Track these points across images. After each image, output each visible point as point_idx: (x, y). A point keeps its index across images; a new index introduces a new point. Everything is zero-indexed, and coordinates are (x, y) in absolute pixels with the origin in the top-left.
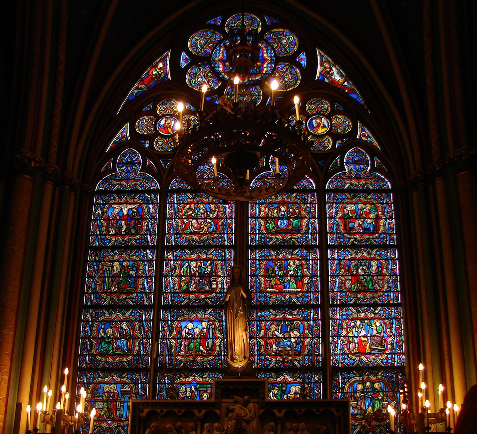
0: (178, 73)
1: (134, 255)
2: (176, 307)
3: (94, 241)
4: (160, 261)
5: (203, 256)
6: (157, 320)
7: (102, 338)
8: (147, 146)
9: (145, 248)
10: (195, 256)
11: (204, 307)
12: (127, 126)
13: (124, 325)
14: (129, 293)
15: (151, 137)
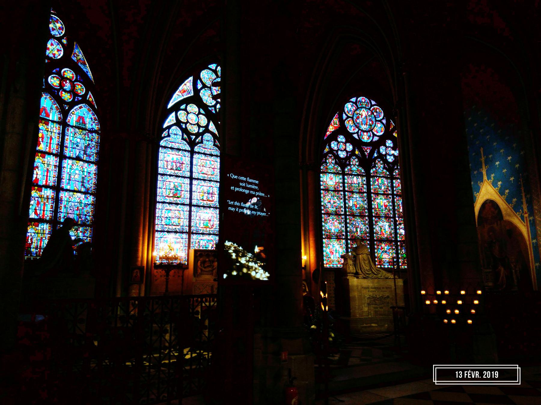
0: (197, 91)
1: (179, 180)
2: (197, 206)
3: (160, 171)
4: (191, 184)
5: (209, 185)
6: (190, 211)
7: (167, 217)
8: (184, 127)
9: (185, 177)
10: (206, 184)
11: (210, 207)
12: (173, 114)
13: (176, 212)
14: (178, 198)
15: (186, 123)
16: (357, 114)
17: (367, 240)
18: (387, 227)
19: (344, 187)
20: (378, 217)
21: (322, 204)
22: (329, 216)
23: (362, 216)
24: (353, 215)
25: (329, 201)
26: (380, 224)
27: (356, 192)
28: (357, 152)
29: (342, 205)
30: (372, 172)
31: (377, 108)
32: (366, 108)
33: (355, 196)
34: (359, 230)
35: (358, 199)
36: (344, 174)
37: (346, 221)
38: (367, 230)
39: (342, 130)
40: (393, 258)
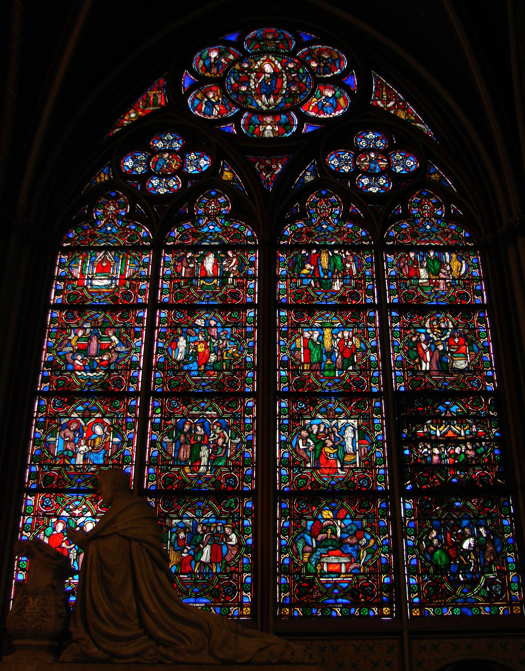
16: (242, 70)
17: (244, 494)
18: (349, 434)
19: (154, 289)
20: (307, 396)
21: (46, 356)
22: (70, 403)
23: (226, 395)
24: (186, 396)
25: (74, 349)
26: (318, 424)
27: (209, 308)
28: (228, 175)
29: (138, 357)
30: (288, 231)
31: (321, 51)
32: (276, 54)
33: (200, 322)
34: (204, 452)
35: (214, 332)
36: (158, 246)
37: (144, 419)
38: (249, 453)
39: (175, 117)
40: (375, 570)
